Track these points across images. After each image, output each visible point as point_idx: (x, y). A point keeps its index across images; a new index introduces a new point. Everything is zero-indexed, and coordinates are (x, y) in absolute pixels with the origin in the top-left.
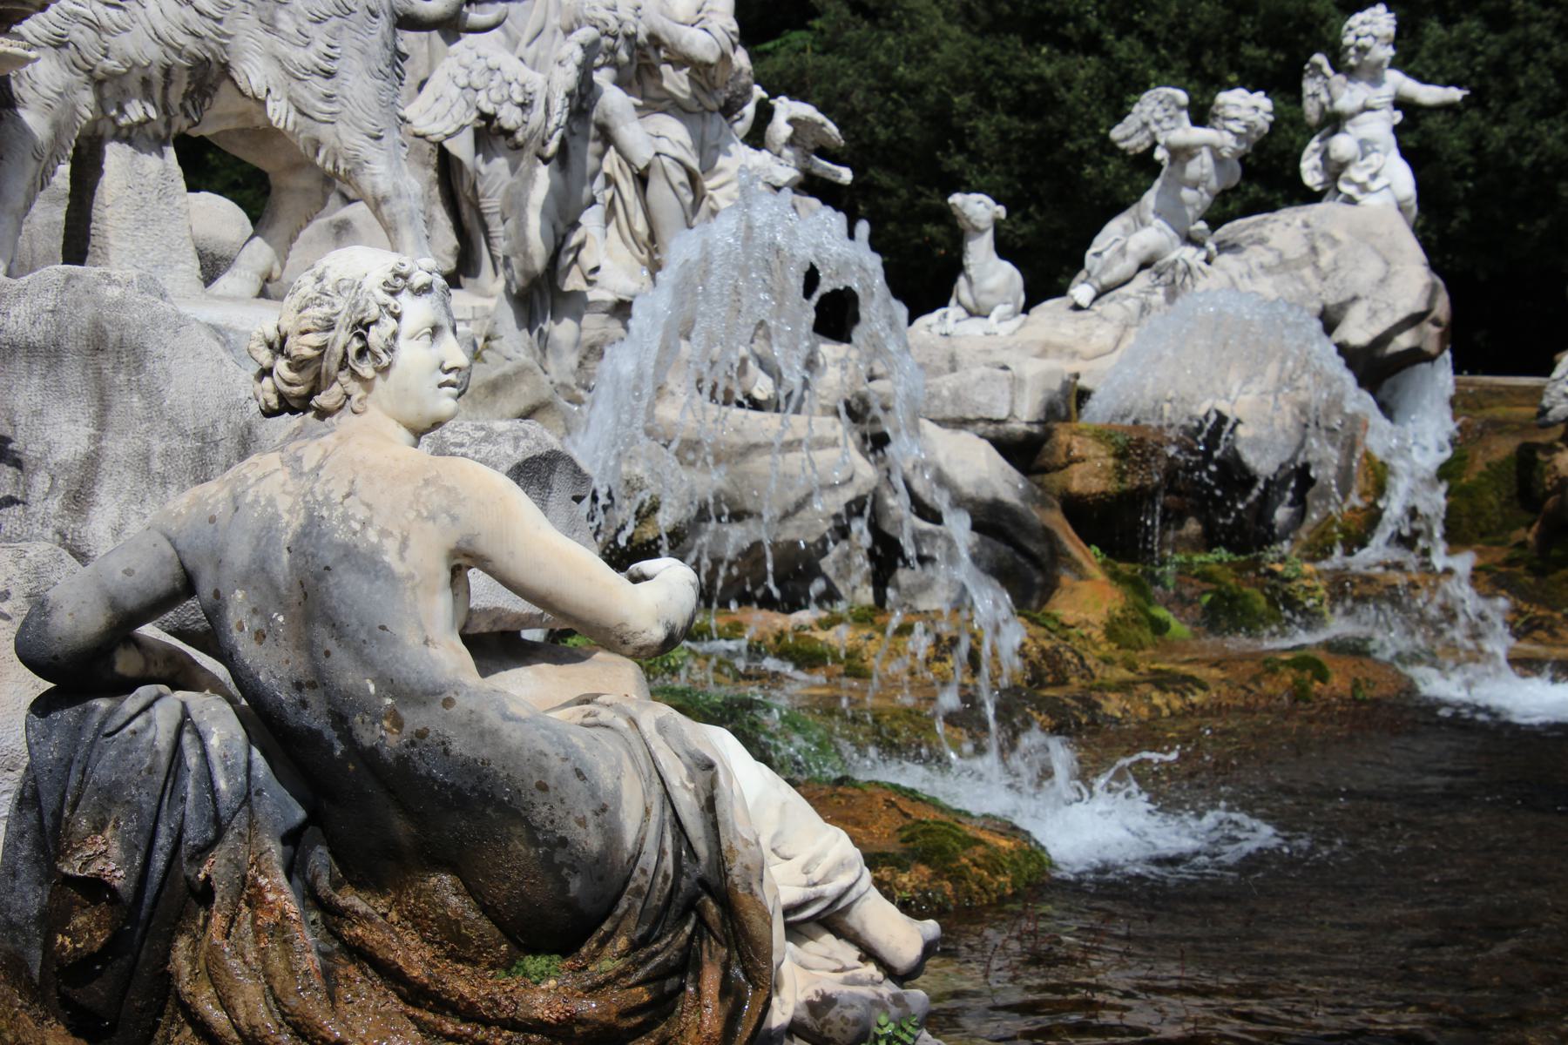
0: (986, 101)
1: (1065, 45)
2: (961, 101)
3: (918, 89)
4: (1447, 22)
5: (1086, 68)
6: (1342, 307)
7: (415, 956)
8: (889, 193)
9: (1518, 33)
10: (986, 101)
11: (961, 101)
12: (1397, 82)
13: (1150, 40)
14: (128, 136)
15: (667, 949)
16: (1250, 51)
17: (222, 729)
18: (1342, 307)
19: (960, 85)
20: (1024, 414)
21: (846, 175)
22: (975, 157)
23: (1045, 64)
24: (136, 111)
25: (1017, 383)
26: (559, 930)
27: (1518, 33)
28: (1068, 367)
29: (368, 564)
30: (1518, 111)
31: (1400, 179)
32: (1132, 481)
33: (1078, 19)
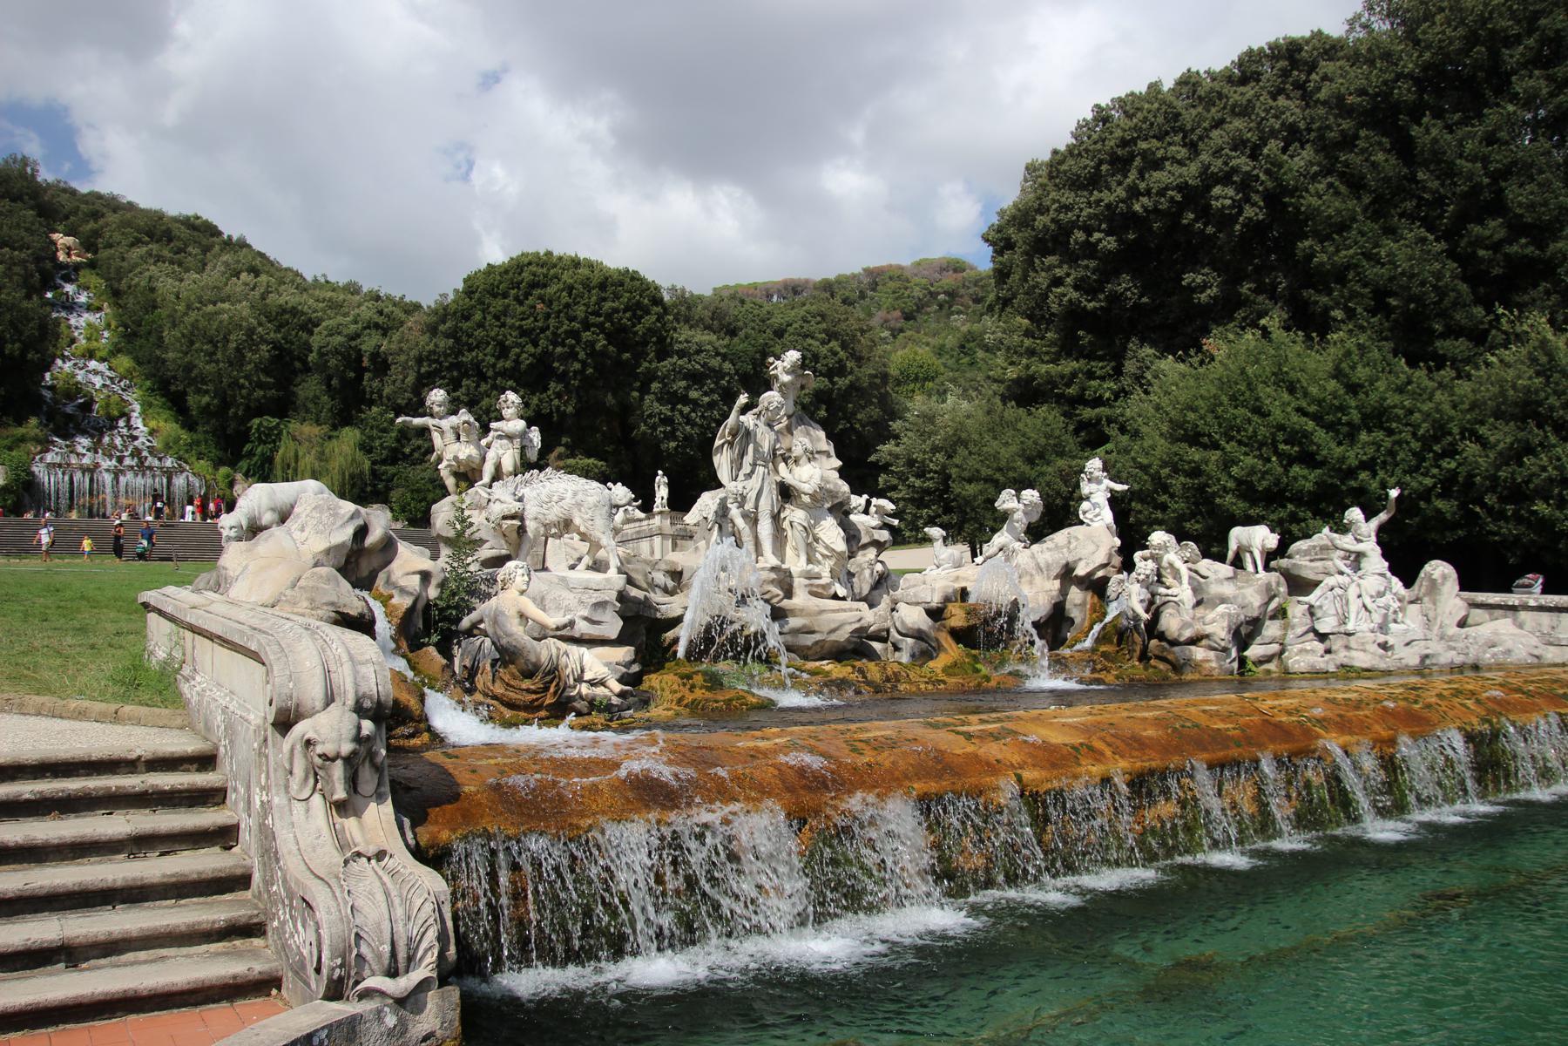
0: (1176, 470)
1: (1205, 447)
2: (1165, 471)
3: (1149, 466)
4: (1370, 431)
5: (1215, 456)
6: (1076, 562)
7: (507, 678)
8: (1140, 512)
9: (1396, 437)
10: (1176, 470)
11: (1165, 471)
12: (1107, 483)
13: (1240, 443)
14: (553, 536)
15: (548, 678)
16: (1282, 447)
17: (488, 642)
18: (1076, 562)
19: (1164, 464)
20: (935, 600)
21: (896, 522)
22: (1172, 496)
23: (1195, 454)
24: (554, 531)
25: (933, 590)
26: (529, 675)
27: (1396, 437)
28: (963, 584)
29: (503, 613)
30: (1398, 471)
31: (1108, 515)
32: (972, 622)
33: (1209, 436)
